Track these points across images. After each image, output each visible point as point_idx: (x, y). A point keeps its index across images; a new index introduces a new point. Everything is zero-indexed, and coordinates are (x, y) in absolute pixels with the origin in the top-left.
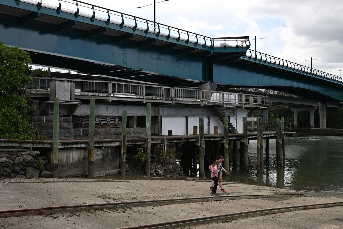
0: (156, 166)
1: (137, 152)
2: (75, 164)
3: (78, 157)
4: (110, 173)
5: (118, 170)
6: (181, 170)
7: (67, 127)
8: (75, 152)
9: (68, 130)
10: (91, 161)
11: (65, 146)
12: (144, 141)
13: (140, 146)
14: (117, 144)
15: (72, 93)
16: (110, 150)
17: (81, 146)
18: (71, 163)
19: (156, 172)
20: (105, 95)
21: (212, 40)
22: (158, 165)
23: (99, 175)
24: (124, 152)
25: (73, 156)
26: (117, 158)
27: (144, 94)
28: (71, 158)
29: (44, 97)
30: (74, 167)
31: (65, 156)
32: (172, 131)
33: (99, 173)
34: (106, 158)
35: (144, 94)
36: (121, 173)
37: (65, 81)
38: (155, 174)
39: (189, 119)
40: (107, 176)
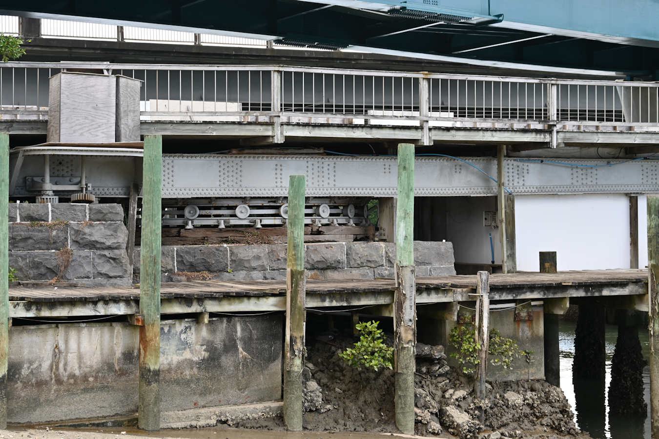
0: (444, 391)
1: (353, 338)
2: (91, 379)
3: (102, 349)
4: (241, 415)
5: (275, 405)
7: (102, 240)
8: (90, 335)
9: (106, 253)
10: (149, 370)
11: (38, 310)
12: (390, 293)
13: (368, 313)
14: (268, 305)
15: (122, 115)
16: (239, 328)
17: (109, 313)
18: (72, 376)
19: (441, 415)
20: (263, 118)
22: (451, 391)
23: (189, 423)
24: (295, 334)
25: (82, 350)
26: (271, 359)
28: (72, 359)
29: (28, 133)
30: (86, 390)
31: (49, 348)
32: (556, 252)
33: (191, 412)
34: (223, 358)
36: (285, 418)
37: (106, 73)
38: (436, 426)
40: (225, 425)
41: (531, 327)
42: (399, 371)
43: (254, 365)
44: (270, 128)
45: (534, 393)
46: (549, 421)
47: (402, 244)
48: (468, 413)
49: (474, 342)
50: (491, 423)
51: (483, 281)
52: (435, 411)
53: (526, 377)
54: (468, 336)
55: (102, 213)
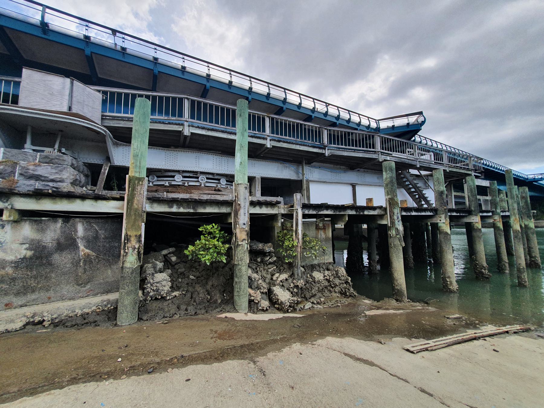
6: (347, 282)
19: (269, 294)
21: (377, 122)
22: (277, 275)
24: (129, 233)
38: (265, 304)
39: (358, 188)
41: (325, 233)
42: (235, 263)
43: (99, 261)
44: (182, 127)
45: (329, 272)
46: (339, 289)
47: (238, 168)
48: (289, 290)
49: (293, 240)
50: (305, 295)
51: (298, 199)
52: (266, 290)
53: (323, 261)
54: (289, 236)
55: (49, 158)
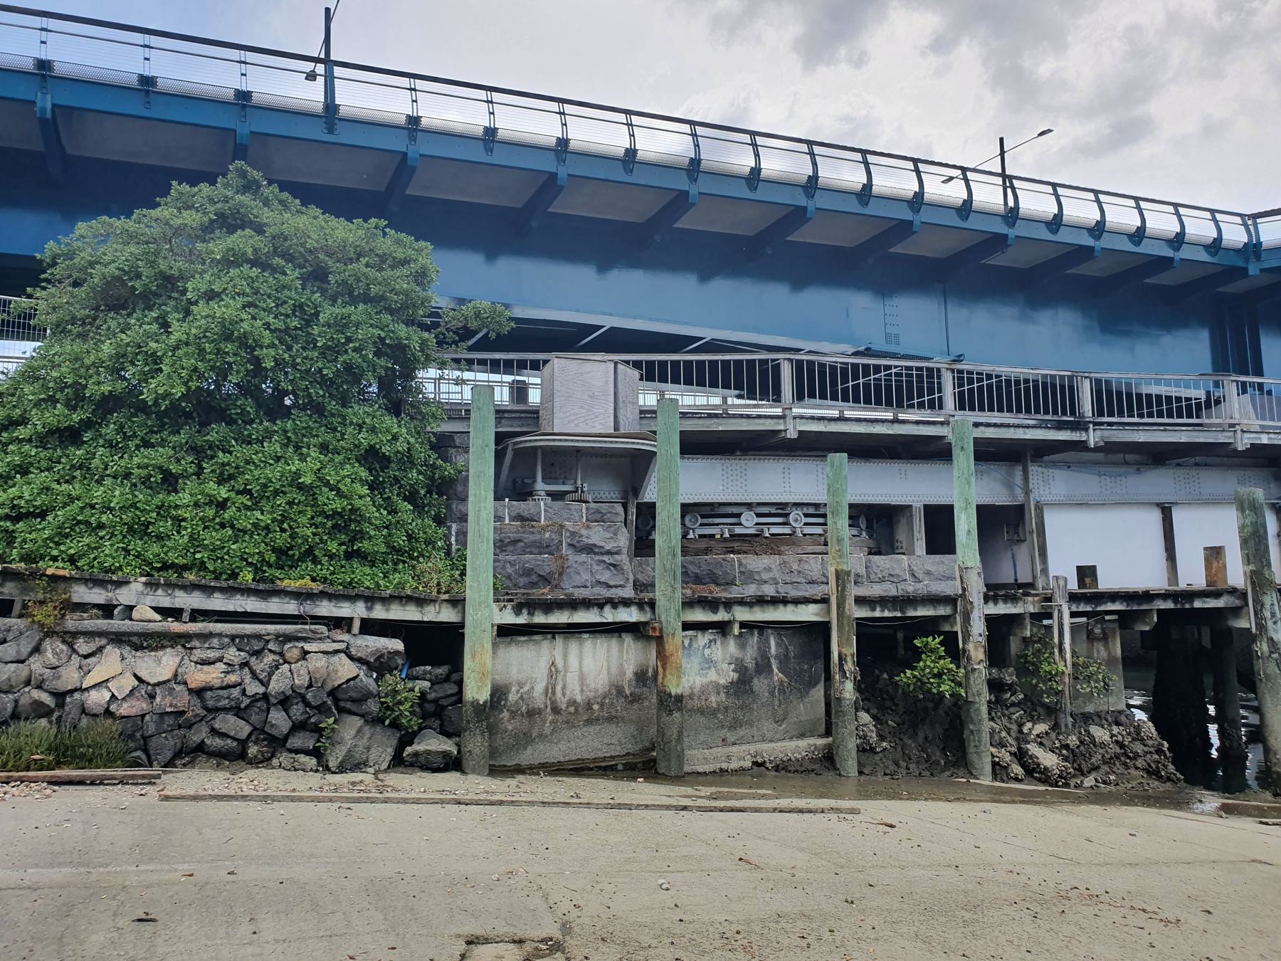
0: (1021, 725)
2: (596, 707)
3: (609, 668)
4: (781, 755)
5: (821, 742)
6: (1159, 751)
8: (595, 648)
9: (605, 558)
10: (670, 695)
11: (531, 614)
12: (950, 600)
13: (929, 626)
14: (808, 613)
15: (621, 405)
17: (618, 620)
18: (572, 703)
21: (1250, 222)
22: (1029, 725)
24: (844, 651)
26: (812, 683)
27: (949, 402)
30: (589, 722)
32: (1094, 567)
33: (720, 751)
34: (755, 681)
35: (949, 402)
36: (837, 759)
38: (1017, 769)
39: (1178, 516)
41: (1107, 647)
42: (969, 700)
43: (792, 690)
44: (782, 421)
45: (1121, 728)
46: (1144, 763)
47: (965, 540)
48: (1053, 752)
49: (1055, 663)
50: (1079, 765)
51: (1061, 587)
52: (1014, 749)
53: (1106, 708)
54: (1046, 655)
55: (601, 513)
